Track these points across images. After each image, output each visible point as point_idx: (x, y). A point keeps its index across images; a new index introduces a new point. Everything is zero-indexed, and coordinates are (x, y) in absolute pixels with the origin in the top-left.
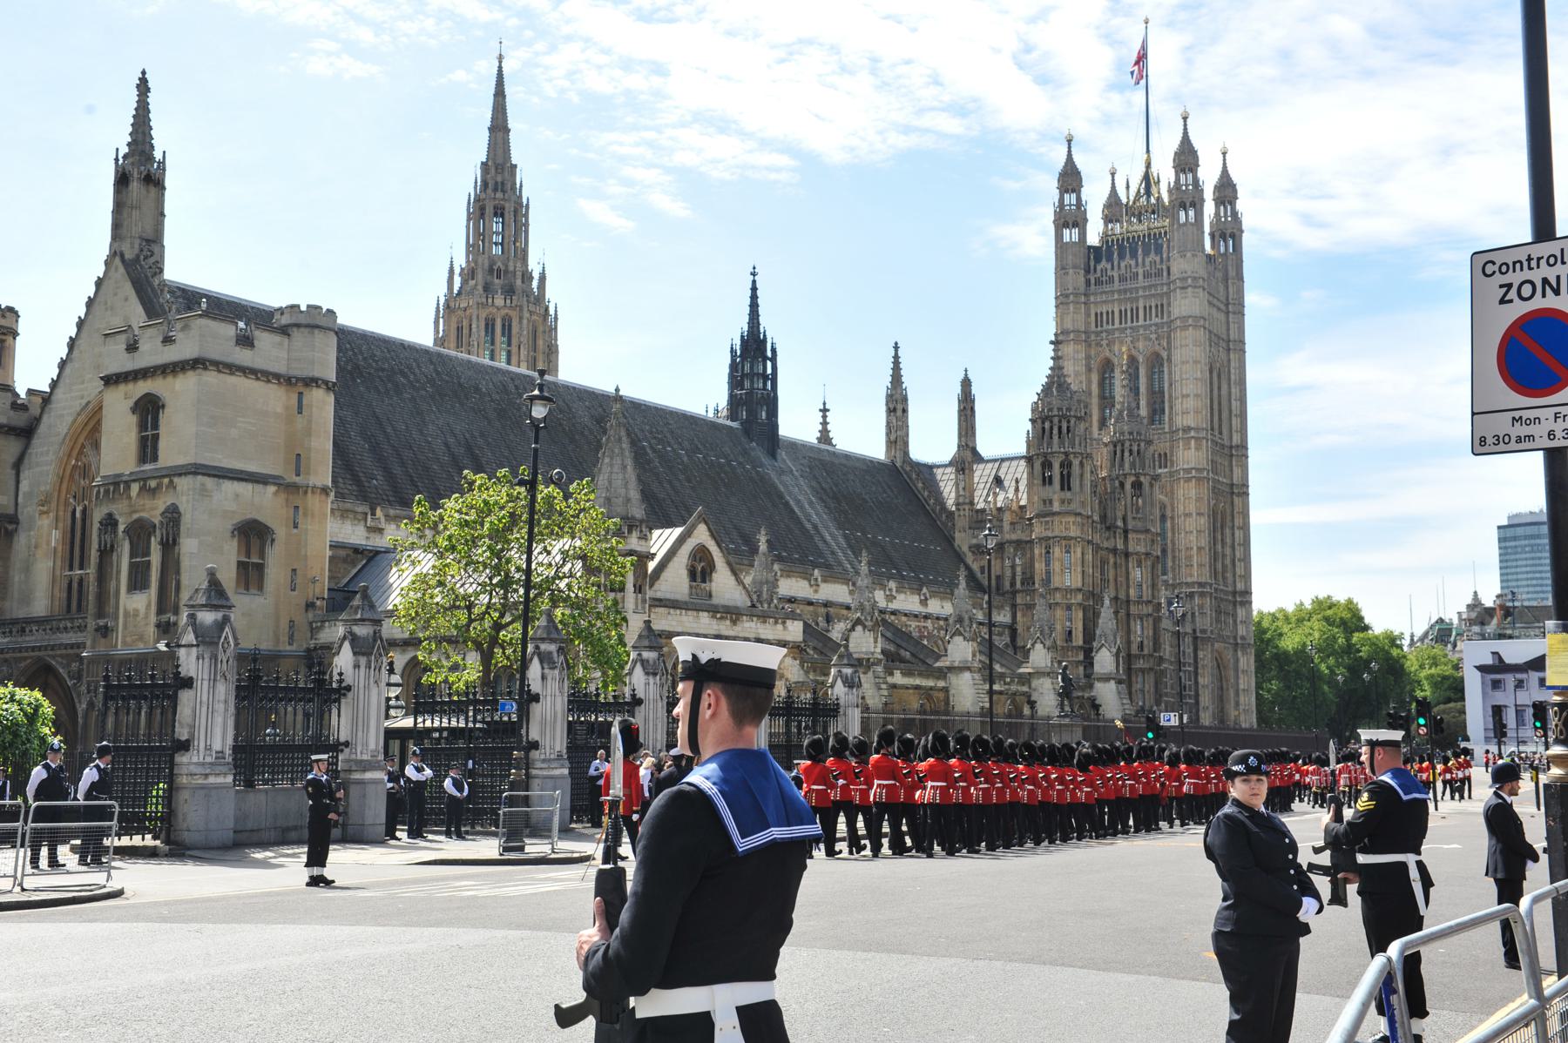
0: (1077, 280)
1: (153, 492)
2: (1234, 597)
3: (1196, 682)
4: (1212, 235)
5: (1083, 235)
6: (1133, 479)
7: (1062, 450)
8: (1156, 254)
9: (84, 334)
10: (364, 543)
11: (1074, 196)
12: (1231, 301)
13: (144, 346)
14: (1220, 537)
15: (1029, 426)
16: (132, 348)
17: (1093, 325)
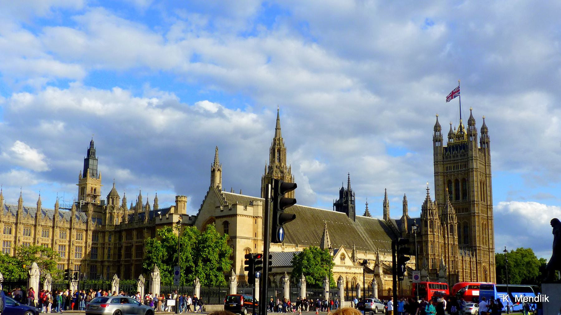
0: (440, 157)
4: (481, 143)
5: (441, 144)
7: (430, 218)
8: (463, 149)
12: (486, 162)
13: (225, 211)
14: (484, 232)
17: (445, 170)
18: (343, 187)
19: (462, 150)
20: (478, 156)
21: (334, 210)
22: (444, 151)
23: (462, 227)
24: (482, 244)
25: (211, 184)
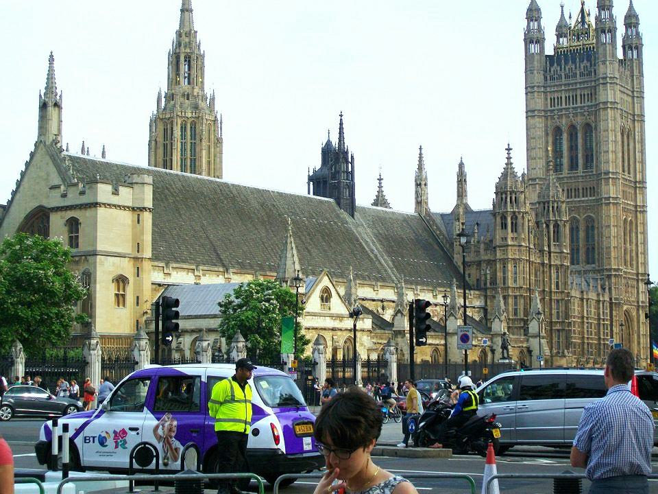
0: (538, 78)
1: (77, 263)
2: (638, 276)
3: (612, 330)
4: (624, 47)
5: (542, 49)
6: (554, 223)
7: (512, 210)
8: (588, 61)
9: (26, 179)
10: (163, 281)
11: (536, 23)
12: (635, 90)
13: (70, 196)
14: (628, 239)
15: (494, 196)
16: (64, 196)
18: (329, 141)
19: (585, 61)
20: (617, 75)
21: (309, 193)
22: (546, 63)
23: (582, 227)
24: (623, 264)
25: (40, 135)
